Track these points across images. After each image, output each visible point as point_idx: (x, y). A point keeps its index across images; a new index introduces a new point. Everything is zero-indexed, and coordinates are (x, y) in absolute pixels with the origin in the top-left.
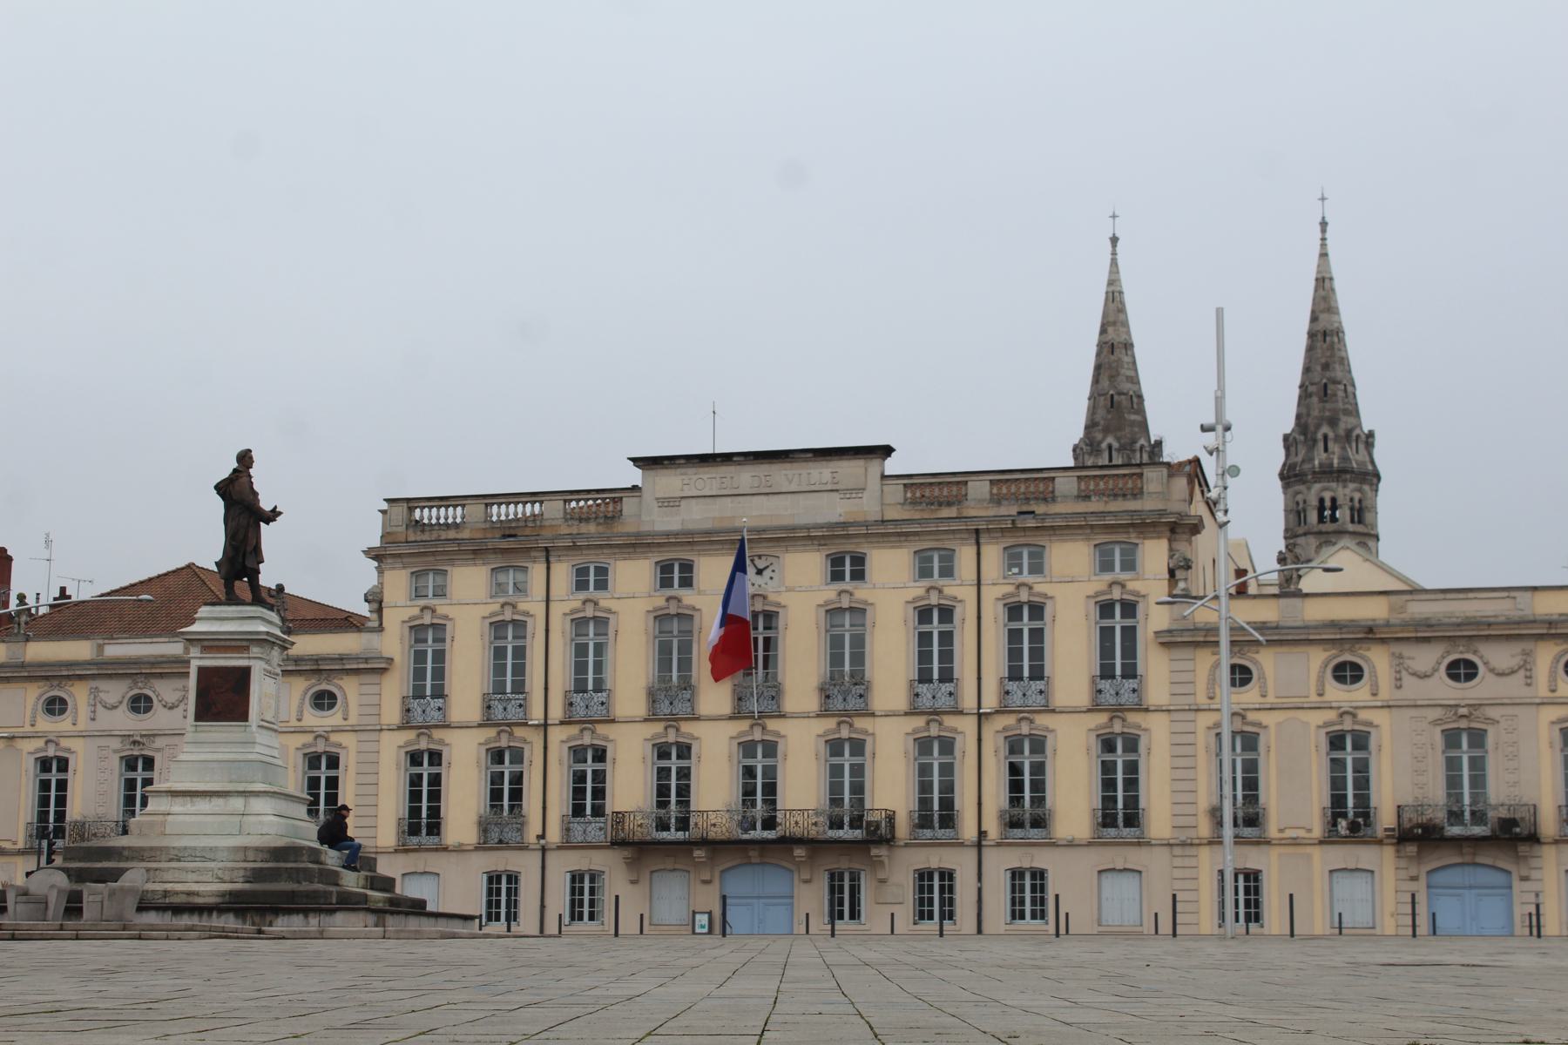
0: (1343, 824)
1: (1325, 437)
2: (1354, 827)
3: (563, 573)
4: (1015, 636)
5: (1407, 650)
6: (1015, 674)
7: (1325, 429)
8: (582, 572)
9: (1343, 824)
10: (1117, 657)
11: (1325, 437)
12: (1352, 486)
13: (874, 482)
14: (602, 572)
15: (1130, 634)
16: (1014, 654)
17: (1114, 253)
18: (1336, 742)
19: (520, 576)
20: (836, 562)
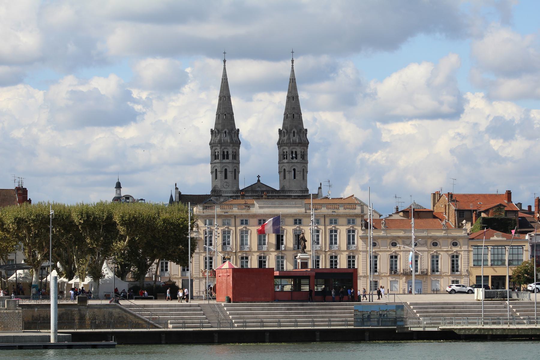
0: (393, 272)
1: (294, 132)
2: (395, 273)
3: (238, 221)
4: (331, 236)
5: (405, 240)
6: (331, 243)
7: (294, 130)
8: (242, 221)
9: (393, 272)
10: (350, 240)
11: (294, 132)
12: (302, 148)
13: (304, 205)
14: (246, 221)
15: (353, 236)
16: (331, 240)
17: (225, 66)
18: (392, 257)
19: (228, 221)
20: (296, 220)
